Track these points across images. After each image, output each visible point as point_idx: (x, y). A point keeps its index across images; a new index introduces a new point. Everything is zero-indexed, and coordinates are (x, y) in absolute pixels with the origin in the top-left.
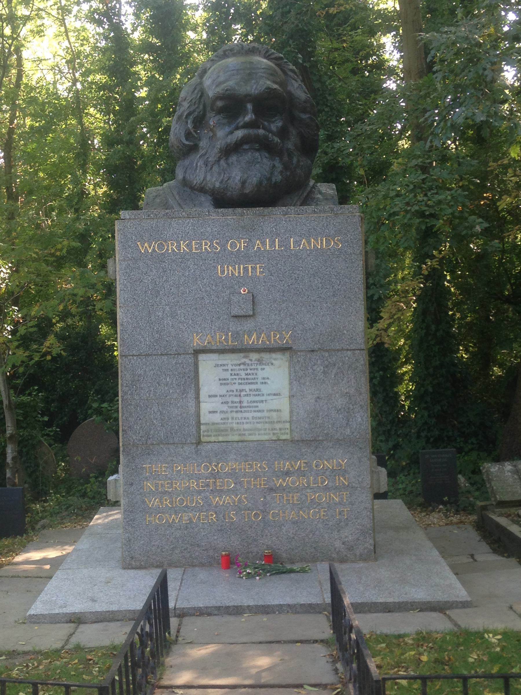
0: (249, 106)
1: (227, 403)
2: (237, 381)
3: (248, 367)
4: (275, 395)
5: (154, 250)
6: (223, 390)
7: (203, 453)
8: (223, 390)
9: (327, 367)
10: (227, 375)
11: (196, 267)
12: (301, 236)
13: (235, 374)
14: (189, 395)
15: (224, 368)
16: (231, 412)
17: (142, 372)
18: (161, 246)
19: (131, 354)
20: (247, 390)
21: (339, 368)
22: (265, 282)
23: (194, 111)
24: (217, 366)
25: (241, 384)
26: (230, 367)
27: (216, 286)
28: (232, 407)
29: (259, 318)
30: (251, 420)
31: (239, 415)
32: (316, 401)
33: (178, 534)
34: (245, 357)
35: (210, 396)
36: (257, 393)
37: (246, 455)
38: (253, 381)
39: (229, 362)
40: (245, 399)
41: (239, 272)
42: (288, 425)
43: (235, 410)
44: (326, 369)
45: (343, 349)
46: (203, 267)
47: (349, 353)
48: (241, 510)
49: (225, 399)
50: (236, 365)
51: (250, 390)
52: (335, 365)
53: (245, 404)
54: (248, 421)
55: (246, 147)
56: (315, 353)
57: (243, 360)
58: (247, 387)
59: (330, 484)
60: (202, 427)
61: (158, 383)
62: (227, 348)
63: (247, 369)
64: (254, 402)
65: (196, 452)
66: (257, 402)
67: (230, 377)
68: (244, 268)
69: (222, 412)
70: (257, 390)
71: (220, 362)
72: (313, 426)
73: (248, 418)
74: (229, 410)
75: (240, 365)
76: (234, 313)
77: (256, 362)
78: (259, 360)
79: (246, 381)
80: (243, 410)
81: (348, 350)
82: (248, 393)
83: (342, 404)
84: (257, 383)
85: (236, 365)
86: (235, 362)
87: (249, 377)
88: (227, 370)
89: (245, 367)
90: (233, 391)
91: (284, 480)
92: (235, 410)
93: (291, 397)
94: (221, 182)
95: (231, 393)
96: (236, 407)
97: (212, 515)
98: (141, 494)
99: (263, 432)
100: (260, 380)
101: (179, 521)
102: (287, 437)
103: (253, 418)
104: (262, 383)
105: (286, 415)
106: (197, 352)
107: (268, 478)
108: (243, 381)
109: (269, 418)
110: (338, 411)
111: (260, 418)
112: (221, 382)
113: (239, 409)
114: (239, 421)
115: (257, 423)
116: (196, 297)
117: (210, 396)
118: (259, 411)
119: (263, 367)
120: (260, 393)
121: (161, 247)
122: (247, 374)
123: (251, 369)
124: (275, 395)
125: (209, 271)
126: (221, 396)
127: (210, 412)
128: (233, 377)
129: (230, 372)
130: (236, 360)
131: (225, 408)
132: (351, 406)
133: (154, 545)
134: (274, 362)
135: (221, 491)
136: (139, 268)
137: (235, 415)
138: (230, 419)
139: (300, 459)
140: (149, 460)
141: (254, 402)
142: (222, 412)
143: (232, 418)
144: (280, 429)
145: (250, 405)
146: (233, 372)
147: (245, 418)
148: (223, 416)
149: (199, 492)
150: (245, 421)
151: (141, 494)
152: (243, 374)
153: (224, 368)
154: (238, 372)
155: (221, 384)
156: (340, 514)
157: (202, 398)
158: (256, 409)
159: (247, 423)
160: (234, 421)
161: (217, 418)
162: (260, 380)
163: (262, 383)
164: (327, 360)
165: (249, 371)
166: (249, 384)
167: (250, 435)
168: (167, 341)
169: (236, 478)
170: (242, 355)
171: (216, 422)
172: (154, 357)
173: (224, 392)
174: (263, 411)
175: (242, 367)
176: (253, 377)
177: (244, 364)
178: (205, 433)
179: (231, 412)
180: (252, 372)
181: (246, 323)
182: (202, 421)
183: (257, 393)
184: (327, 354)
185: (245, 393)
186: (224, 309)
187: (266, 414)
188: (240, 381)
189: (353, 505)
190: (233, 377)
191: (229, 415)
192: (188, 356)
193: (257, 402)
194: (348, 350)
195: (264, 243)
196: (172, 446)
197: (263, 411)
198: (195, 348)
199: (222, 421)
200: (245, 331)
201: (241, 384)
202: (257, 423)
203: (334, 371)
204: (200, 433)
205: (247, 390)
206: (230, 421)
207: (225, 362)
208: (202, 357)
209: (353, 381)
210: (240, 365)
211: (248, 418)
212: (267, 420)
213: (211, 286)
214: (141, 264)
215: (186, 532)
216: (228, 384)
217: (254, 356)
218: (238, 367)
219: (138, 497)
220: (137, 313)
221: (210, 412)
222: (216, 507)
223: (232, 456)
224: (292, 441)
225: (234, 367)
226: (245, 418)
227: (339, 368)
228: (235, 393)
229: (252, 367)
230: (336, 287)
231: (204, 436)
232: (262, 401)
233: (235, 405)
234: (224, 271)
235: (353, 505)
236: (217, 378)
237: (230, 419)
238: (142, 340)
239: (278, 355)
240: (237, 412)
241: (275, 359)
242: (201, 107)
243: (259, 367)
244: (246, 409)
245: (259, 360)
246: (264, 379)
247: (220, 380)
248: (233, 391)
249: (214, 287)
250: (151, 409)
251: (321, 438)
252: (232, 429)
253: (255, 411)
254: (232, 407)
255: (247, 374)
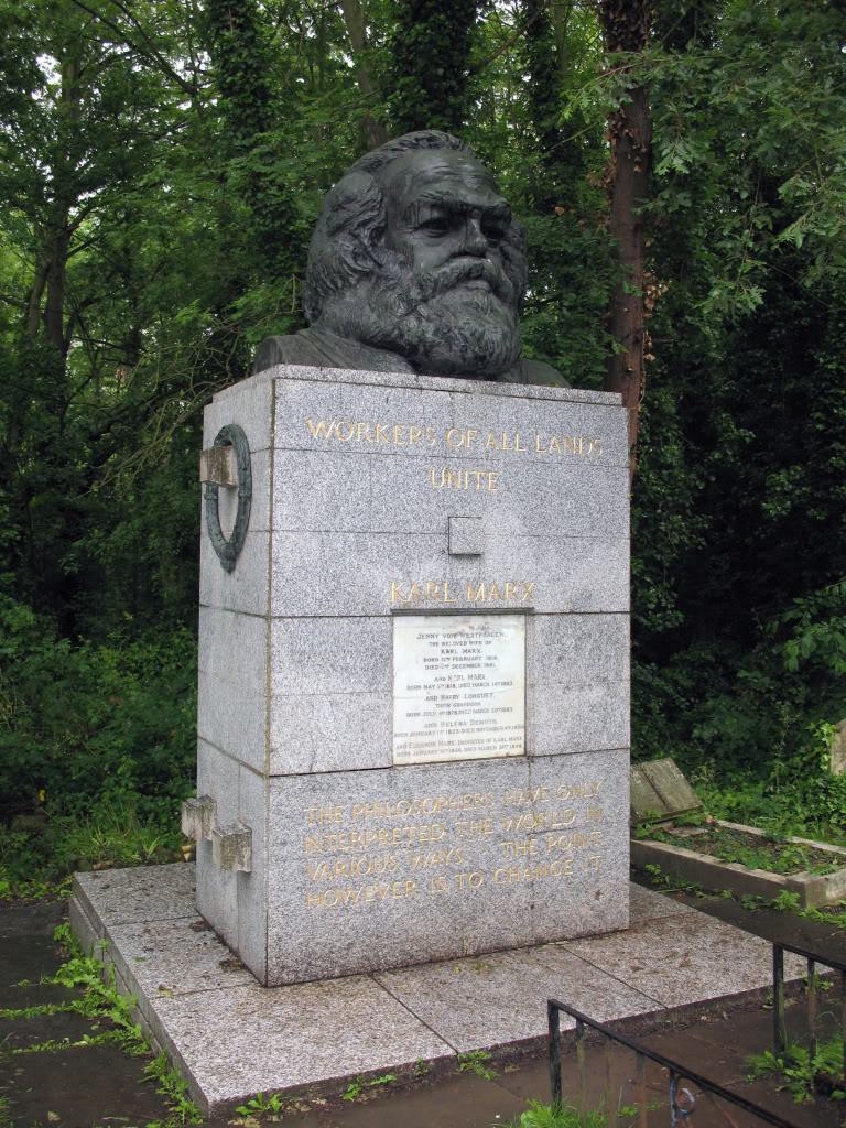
0: (475, 223)
1: (434, 698)
2: (451, 663)
3: (467, 640)
4: (504, 684)
5: (333, 436)
6: (427, 677)
7: (400, 785)
8: (427, 677)
9: (580, 638)
10: (436, 652)
11: (399, 469)
12: (550, 432)
13: (448, 652)
14: (381, 687)
15: (432, 640)
16: (441, 713)
17: (307, 647)
18: (345, 429)
19: (289, 614)
20: (465, 677)
21: (595, 641)
22: (500, 501)
23: (371, 220)
24: (421, 636)
25: (456, 666)
26: (441, 639)
27: (428, 502)
28: (442, 706)
29: (490, 560)
30: (468, 726)
31: (453, 718)
32: (564, 693)
33: (357, 921)
34: (465, 622)
35: (409, 688)
36: (480, 681)
37: (465, 784)
38: (474, 662)
39: (441, 631)
40: (461, 692)
41: (463, 483)
42: (521, 733)
43: (446, 709)
44: (578, 643)
45: (601, 612)
46: (409, 471)
47: (609, 617)
48: (454, 872)
49: (434, 692)
50: (449, 636)
51: (470, 677)
52: (590, 636)
53: (461, 701)
54: (464, 727)
55: (472, 284)
56: (566, 617)
57: (460, 629)
58: (465, 672)
59: (578, 821)
60: (397, 741)
61: (332, 666)
62: (442, 606)
63: (465, 643)
64: (474, 696)
65: (389, 783)
66: (478, 696)
67: (440, 656)
68: (470, 476)
69: (426, 714)
70: (479, 677)
71: (426, 632)
72: (558, 732)
73: (465, 723)
74: (439, 710)
75: (455, 635)
76: (455, 550)
77: (479, 631)
78: (483, 628)
79: (465, 662)
80: (458, 709)
81: (607, 613)
82: (466, 681)
83: (598, 697)
84: (479, 665)
85: (449, 636)
86: (446, 632)
87: (468, 655)
88: (436, 644)
89: (462, 639)
90: (444, 679)
91: (515, 820)
92: (446, 709)
93: (529, 687)
94: (435, 333)
95: (442, 682)
96: (449, 706)
97: (411, 885)
98: (299, 859)
99: (485, 745)
100: (483, 661)
101: (360, 900)
102: (520, 751)
103: (473, 722)
104: (487, 665)
105: (518, 717)
106: (396, 613)
107: (494, 819)
108: (459, 663)
109: (495, 721)
110: (593, 707)
111: (482, 722)
112: (427, 663)
113: (452, 708)
114: (452, 729)
115: (478, 730)
116: (398, 519)
117: (409, 688)
118: (481, 711)
119: (490, 639)
120: (483, 681)
121: (344, 429)
122: (465, 651)
123: (471, 643)
124: (504, 684)
125: (418, 477)
126: (426, 687)
127: (409, 715)
128: (444, 656)
129: (440, 647)
130: (451, 627)
131: (431, 707)
132: (609, 699)
133: (318, 943)
134: (504, 630)
135: (427, 844)
136: (307, 465)
137: (445, 718)
138: (439, 724)
139: (539, 786)
140: (314, 800)
141: (474, 696)
142: (426, 714)
143: (443, 724)
144: (511, 739)
145: (469, 700)
146: (445, 648)
147: (461, 723)
148: (429, 720)
149: (393, 850)
150: (460, 728)
151: (299, 859)
152: (459, 649)
153: (432, 640)
154: (452, 647)
155: (427, 667)
156: (590, 865)
157: (396, 692)
158: (477, 708)
159: (463, 731)
160: (445, 728)
161: (418, 724)
162: (483, 661)
163: (487, 665)
164: (581, 629)
165: (468, 646)
166: (468, 666)
167: (466, 750)
168: (349, 594)
169: (449, 823)
170: (459, 618)
171: (417, 731)
172: (327, 620)
173: (432, 682)
174: (487, 711)
175: (459, 639)
176: (474, 655)
177: (462, 634)
178: (400, 751)
179: (441, 713)
180: (474, 646)
181: (470, 566)
182: (396, 731)
183: (480, 681)
184: (579, 619)
185: (461, 682)
186: (439, 541)
187: (491, 715)
188: (455, 663)
189: (605, 849)
190: (444, 656)
191: (438, 720)
192: (380, 620)
193: (478, 696)
194: (607, 613)
195: (499, 438)
196: (352, 774)
197: (487, 711)
198: (392, 607)
199: (425, 730)
200: (468, 580)
201: (456, 666)
202: (478, 730)
203: (589, 646)
204: (392, 751)
205: (465, 677)
206: (439, 728)
207: (434, 631)
208: (399, 622)
209: (613, 660)
210: (455, 635)
211: (465, 723)
212: (492, 725)
213: (420, 502)
214: (311, 456)
215: (370, 916)
216: (437, 667)
217: (477, 621)
218: (452, 640)
219: (295, 864)
220: (302, 543)
221: (409, 715)
222: (416, 871)
223: (444, 787)
224: (529, 757)
225: (447, 639)
226: (461, 723)
227: (595, 641)
228: (447, 682)
229: (472, 640)
230: (595, 515)
231: (398, 755)
232: (486, 695)
233: (447, 701)
234: (441, 478)
235: (605, 849)
236: (421, 660)
237: (439, 724)
238: (309, 590)
239: (511, 621)
240: (449, 713)
241: (508, 627)
242: (383, 213)
243: (482, 639)
244: (461, 708)
245: (483, 628)
246: (489, 658)
247: (425, 660)
248: (444, 679)
249: (425, 506)
250: (319, 711)
251: (569, 751)
252: (441, 743)
253: (476, 712)
254: (442, 706)
255: (465, 651)
